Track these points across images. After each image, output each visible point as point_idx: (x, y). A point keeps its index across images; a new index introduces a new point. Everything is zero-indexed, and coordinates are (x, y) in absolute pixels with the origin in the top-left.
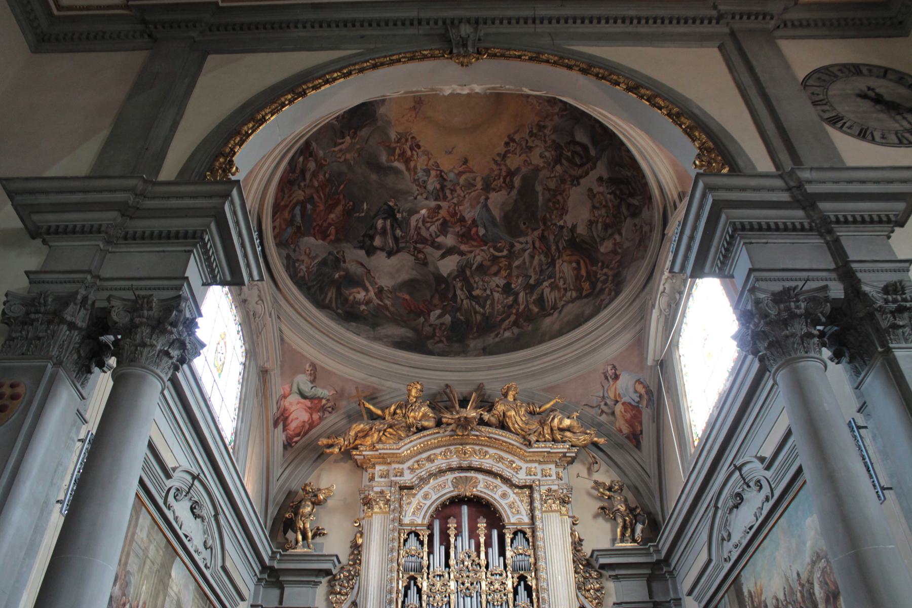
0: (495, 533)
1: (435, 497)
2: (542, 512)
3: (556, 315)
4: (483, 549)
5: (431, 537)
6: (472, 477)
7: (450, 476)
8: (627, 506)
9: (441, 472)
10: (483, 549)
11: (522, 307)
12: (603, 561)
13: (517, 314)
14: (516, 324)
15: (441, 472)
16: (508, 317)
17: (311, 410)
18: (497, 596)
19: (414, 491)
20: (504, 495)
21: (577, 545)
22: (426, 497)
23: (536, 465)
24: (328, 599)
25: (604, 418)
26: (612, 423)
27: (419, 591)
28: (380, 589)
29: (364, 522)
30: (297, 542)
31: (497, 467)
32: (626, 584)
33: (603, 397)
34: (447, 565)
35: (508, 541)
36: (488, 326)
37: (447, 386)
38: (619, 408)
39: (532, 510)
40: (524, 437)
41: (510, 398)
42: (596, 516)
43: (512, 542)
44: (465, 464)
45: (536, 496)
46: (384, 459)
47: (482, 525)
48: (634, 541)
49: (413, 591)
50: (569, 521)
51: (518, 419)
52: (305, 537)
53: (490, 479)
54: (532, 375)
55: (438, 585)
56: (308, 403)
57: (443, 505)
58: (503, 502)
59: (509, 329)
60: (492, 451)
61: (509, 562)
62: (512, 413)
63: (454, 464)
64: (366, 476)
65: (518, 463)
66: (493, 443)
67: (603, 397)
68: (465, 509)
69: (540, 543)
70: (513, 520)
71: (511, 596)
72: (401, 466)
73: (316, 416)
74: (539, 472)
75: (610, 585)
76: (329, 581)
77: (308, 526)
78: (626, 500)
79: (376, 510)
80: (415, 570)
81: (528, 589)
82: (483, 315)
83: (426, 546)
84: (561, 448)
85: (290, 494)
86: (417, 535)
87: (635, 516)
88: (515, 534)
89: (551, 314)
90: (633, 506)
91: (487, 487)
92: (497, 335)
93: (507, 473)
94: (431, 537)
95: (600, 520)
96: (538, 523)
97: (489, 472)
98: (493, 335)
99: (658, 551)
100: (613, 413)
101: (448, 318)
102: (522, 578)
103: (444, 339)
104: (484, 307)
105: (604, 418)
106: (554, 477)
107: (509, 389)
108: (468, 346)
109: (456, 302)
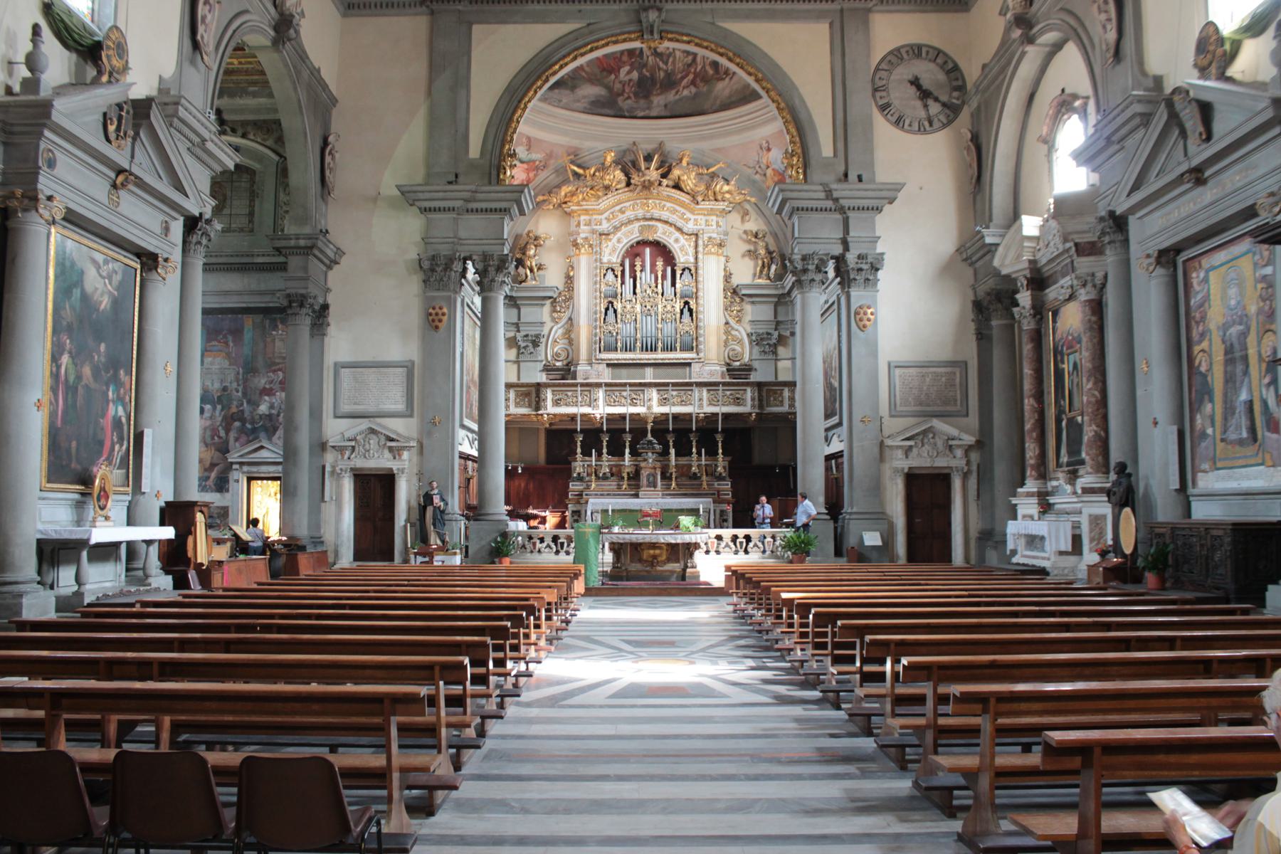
0: (669, 269)
1: (625, 241)
2: (704, 254)
3: (727, 80)
4: (660, 281)
5: (623, 272)
6: (653, 226)
7: (637, 225)
8: (767, 248)
9: (630, 222)
10: (660, 281)
11: (699, 68)
12: (744, 292)
13: (695, 73)
14: (693, 83)
15: (630, 222)
16: (687, 75)
17: (528, 171)
18: (669, 316)
19: (610, 237)
20: (677, 241)
21: (728, 277)
22: (619, 241)
23: (702, 217)
24: (551, 316)
25: (757, 177)
26: (764, 182)
27: (615, 311)
28: (589, 310)
29: (574, 259)
30: (527, 277)
31: (673, 218)
32: (759, 307)
33: (758, 162)
34: (635, 293)
35: (678, 276)
36: (670, 83)
37: (634, 143)
38: (769, 172)
39: (696, 253)
40: (693, 197)
41: (684, 163)
42: (743, 256)
43: (681, 274)
44: (648, 215)
45: (700, 242)
46: (587, 212)
47: (660, 264)
48: (769, 278)
49: (611, 310)
50: (723, 259)
51: (690, 182)
52: (532, 271)
53: (666, 227)
54: (703, 138)
55: (628, 307)
56: (525, 166)
57: (632, 246)
58: (676, 246)
59: (688, 87)
60: (668, 205)
61: (678, 290)
62: (685, 177)
63: (640, 216)
64: (574, 222)
65: (688, 215)
66: (669, 199)
67: (758, 162)
68: (648, 251)
69: (700, 279)
70: (682, 260)
71: (678, 315)
72: (600, 217)
73: (531, 175)
74: (703, 222)
75: (748, 308)
76: (552, 303)
77: (534, 264)
78: (767, 245)
79: (583, 251)
80: (612, 297)
81: (690, 311)
82: (666, 71)
83: (619, 279)
84: (721, 206)
85: (518, 237)
86: (613, 270)
87: (772, 259)
88: (684, 270)
89: (724, 79)
90: (772, 249)
91: (664, 233)
92: (677, 93)
93: (680, 223)
94: (623, 272)
95: (747, 259)
96: (700, 264)
97: (666, 222)
98: (673, 92)
99: (783, 288)
100: (765, 175)
101: (635, 75)
102: (687, 303)
103: (632, 95)
104: (666, 64)
105: (757, 177)
106: (715, 227)
107: (683, 155)
108: (652, 102)
109: (642, 58)
